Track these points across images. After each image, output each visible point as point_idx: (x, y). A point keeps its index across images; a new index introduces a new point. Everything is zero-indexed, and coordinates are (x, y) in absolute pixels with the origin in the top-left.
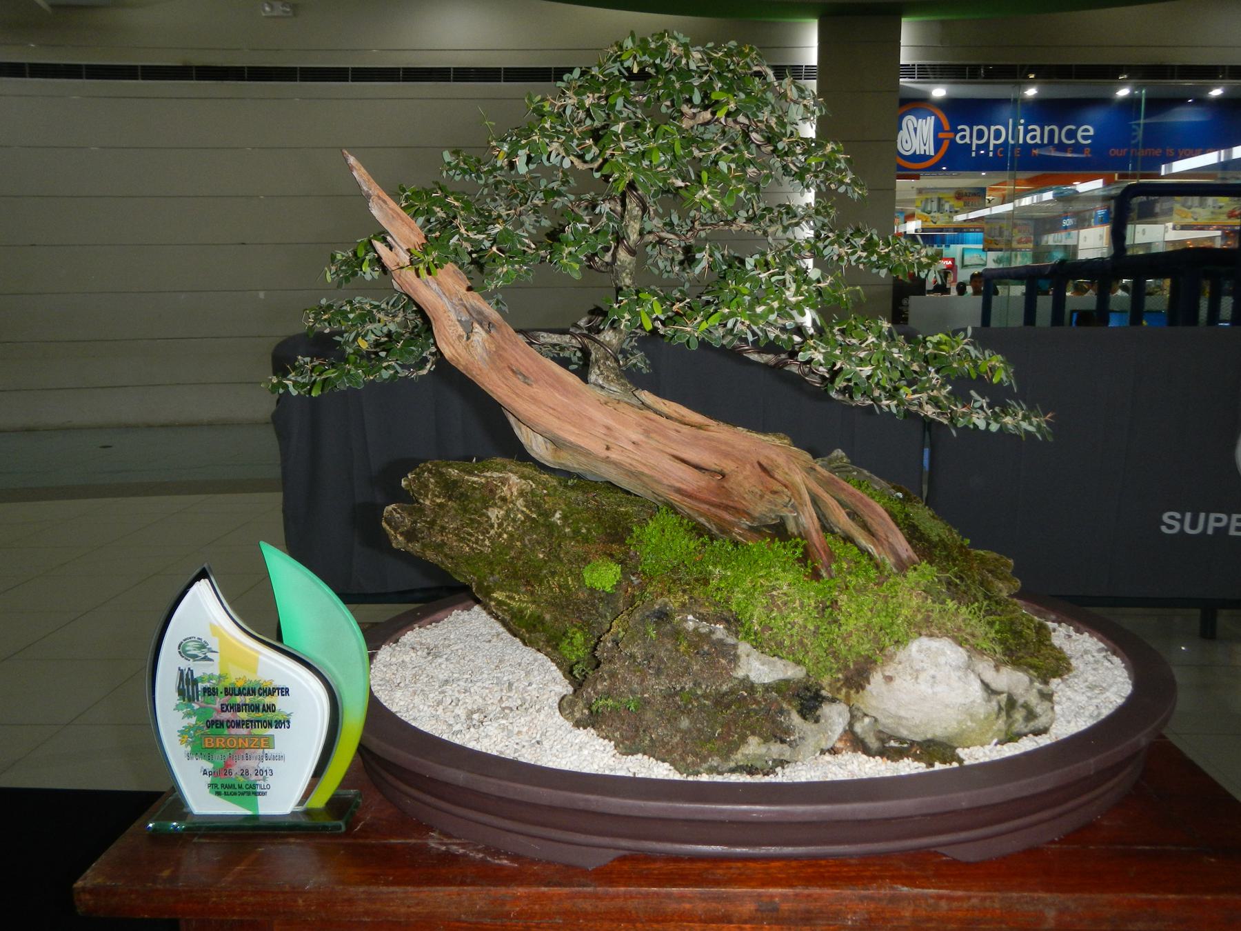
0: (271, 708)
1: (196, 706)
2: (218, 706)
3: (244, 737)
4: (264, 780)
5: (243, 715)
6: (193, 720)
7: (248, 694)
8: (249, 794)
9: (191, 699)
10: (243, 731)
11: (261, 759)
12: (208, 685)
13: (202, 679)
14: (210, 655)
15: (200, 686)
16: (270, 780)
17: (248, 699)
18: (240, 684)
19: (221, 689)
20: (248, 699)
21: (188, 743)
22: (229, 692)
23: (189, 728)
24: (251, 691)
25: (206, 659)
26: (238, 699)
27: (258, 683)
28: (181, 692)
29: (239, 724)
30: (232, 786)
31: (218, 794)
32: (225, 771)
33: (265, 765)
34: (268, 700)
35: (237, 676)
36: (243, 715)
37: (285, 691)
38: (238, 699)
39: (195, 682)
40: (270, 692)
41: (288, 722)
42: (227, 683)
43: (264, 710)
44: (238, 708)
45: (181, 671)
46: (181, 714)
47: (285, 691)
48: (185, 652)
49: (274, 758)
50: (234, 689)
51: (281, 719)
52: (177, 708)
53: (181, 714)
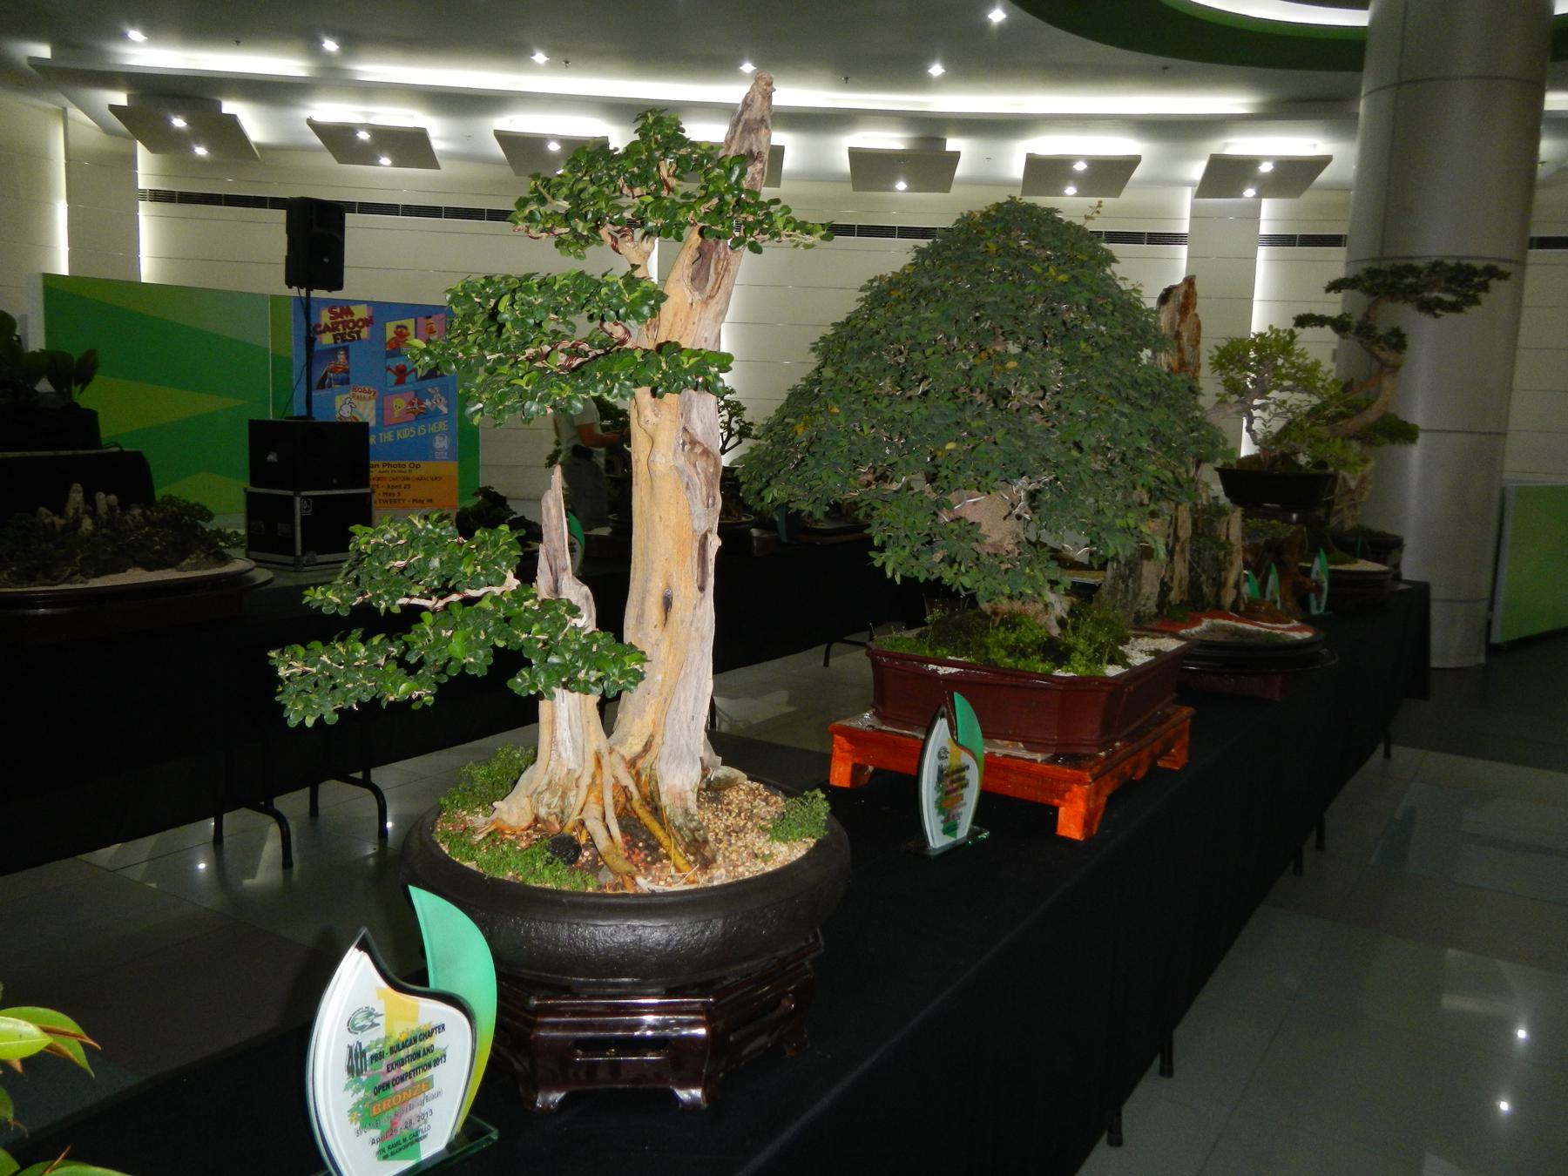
0: (430, 1050)
1: (364, 1078)
2: (384, 1068)
3: (406, 1090)
4: (425, 1122)
5: (407, 1068)
6: (361, 1094)
7: (411, 1044)
8: (412, 1143)
9: (359, 1073)
10: (407, 1083)
11: (422, 1103)
12: (375, 1051)
13: (369, 1048)
14: (376, 1020)
15: (368, 1055)
16: (430, 1120)
17: (410, 1050)
18: (403, 1039)
19: (387, 1050)
20: (410, 1050)
21: (357, 1119)
22: (393, 1050)
23: (358, 1103)
24: (413, 1040)
25: (374, 1025)
26: (402, 1054)
27: (418, 1030)
28: (350, 1070)
29: (402, 1079)
30: (398, 1143)
31: (386, 1157)
32: (391, 1131)
33: (424, 1109)
34: (427, 1043)
35: (400, 1031)
36: (407, 1068)
37: (441, 1028)
38: (402, 1054)
39: (363, 1054)
40: (429, 1034)
41: (445, 1056)
42: (392, 1043)
43: (425, 1054)
44: (402, 1062)
45: (350, 1048)
46: (351, 1092)
47: (441, 1028)
48: (353, 1026)
49: (434, 1097)
50: (398, 1046)
51: (438, 1055)
52: (347, 1088)
53: (351, 1092)
